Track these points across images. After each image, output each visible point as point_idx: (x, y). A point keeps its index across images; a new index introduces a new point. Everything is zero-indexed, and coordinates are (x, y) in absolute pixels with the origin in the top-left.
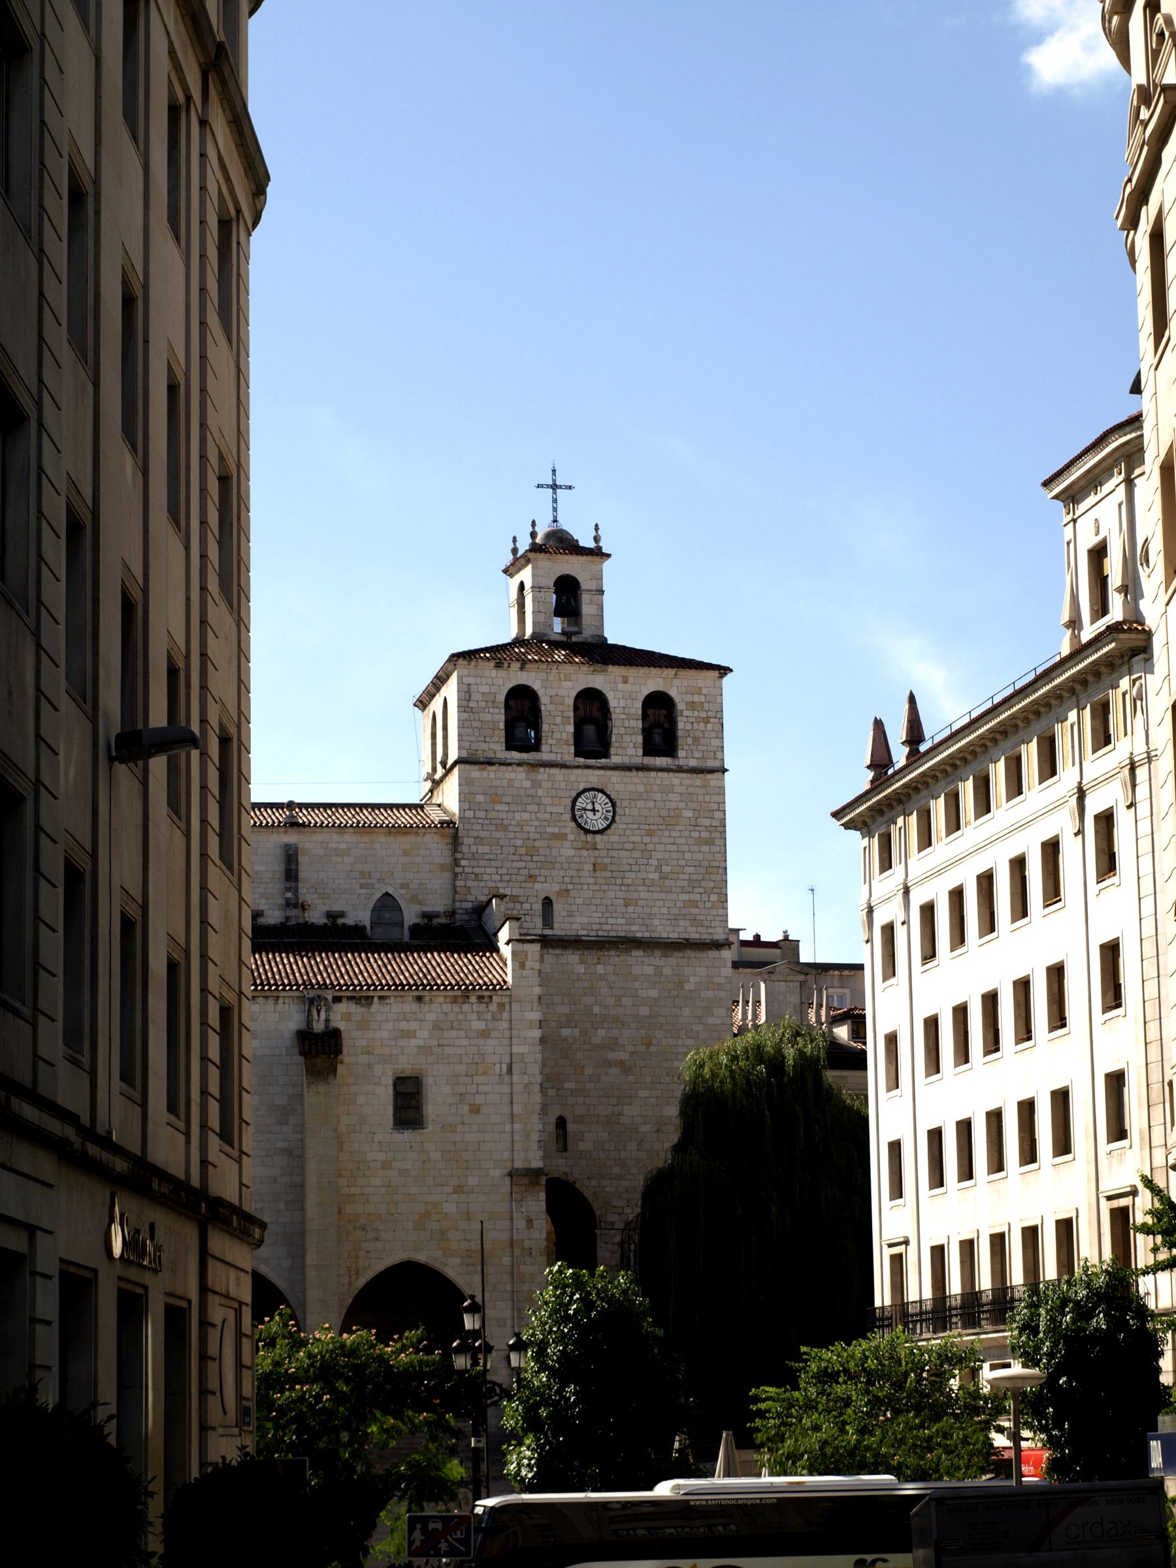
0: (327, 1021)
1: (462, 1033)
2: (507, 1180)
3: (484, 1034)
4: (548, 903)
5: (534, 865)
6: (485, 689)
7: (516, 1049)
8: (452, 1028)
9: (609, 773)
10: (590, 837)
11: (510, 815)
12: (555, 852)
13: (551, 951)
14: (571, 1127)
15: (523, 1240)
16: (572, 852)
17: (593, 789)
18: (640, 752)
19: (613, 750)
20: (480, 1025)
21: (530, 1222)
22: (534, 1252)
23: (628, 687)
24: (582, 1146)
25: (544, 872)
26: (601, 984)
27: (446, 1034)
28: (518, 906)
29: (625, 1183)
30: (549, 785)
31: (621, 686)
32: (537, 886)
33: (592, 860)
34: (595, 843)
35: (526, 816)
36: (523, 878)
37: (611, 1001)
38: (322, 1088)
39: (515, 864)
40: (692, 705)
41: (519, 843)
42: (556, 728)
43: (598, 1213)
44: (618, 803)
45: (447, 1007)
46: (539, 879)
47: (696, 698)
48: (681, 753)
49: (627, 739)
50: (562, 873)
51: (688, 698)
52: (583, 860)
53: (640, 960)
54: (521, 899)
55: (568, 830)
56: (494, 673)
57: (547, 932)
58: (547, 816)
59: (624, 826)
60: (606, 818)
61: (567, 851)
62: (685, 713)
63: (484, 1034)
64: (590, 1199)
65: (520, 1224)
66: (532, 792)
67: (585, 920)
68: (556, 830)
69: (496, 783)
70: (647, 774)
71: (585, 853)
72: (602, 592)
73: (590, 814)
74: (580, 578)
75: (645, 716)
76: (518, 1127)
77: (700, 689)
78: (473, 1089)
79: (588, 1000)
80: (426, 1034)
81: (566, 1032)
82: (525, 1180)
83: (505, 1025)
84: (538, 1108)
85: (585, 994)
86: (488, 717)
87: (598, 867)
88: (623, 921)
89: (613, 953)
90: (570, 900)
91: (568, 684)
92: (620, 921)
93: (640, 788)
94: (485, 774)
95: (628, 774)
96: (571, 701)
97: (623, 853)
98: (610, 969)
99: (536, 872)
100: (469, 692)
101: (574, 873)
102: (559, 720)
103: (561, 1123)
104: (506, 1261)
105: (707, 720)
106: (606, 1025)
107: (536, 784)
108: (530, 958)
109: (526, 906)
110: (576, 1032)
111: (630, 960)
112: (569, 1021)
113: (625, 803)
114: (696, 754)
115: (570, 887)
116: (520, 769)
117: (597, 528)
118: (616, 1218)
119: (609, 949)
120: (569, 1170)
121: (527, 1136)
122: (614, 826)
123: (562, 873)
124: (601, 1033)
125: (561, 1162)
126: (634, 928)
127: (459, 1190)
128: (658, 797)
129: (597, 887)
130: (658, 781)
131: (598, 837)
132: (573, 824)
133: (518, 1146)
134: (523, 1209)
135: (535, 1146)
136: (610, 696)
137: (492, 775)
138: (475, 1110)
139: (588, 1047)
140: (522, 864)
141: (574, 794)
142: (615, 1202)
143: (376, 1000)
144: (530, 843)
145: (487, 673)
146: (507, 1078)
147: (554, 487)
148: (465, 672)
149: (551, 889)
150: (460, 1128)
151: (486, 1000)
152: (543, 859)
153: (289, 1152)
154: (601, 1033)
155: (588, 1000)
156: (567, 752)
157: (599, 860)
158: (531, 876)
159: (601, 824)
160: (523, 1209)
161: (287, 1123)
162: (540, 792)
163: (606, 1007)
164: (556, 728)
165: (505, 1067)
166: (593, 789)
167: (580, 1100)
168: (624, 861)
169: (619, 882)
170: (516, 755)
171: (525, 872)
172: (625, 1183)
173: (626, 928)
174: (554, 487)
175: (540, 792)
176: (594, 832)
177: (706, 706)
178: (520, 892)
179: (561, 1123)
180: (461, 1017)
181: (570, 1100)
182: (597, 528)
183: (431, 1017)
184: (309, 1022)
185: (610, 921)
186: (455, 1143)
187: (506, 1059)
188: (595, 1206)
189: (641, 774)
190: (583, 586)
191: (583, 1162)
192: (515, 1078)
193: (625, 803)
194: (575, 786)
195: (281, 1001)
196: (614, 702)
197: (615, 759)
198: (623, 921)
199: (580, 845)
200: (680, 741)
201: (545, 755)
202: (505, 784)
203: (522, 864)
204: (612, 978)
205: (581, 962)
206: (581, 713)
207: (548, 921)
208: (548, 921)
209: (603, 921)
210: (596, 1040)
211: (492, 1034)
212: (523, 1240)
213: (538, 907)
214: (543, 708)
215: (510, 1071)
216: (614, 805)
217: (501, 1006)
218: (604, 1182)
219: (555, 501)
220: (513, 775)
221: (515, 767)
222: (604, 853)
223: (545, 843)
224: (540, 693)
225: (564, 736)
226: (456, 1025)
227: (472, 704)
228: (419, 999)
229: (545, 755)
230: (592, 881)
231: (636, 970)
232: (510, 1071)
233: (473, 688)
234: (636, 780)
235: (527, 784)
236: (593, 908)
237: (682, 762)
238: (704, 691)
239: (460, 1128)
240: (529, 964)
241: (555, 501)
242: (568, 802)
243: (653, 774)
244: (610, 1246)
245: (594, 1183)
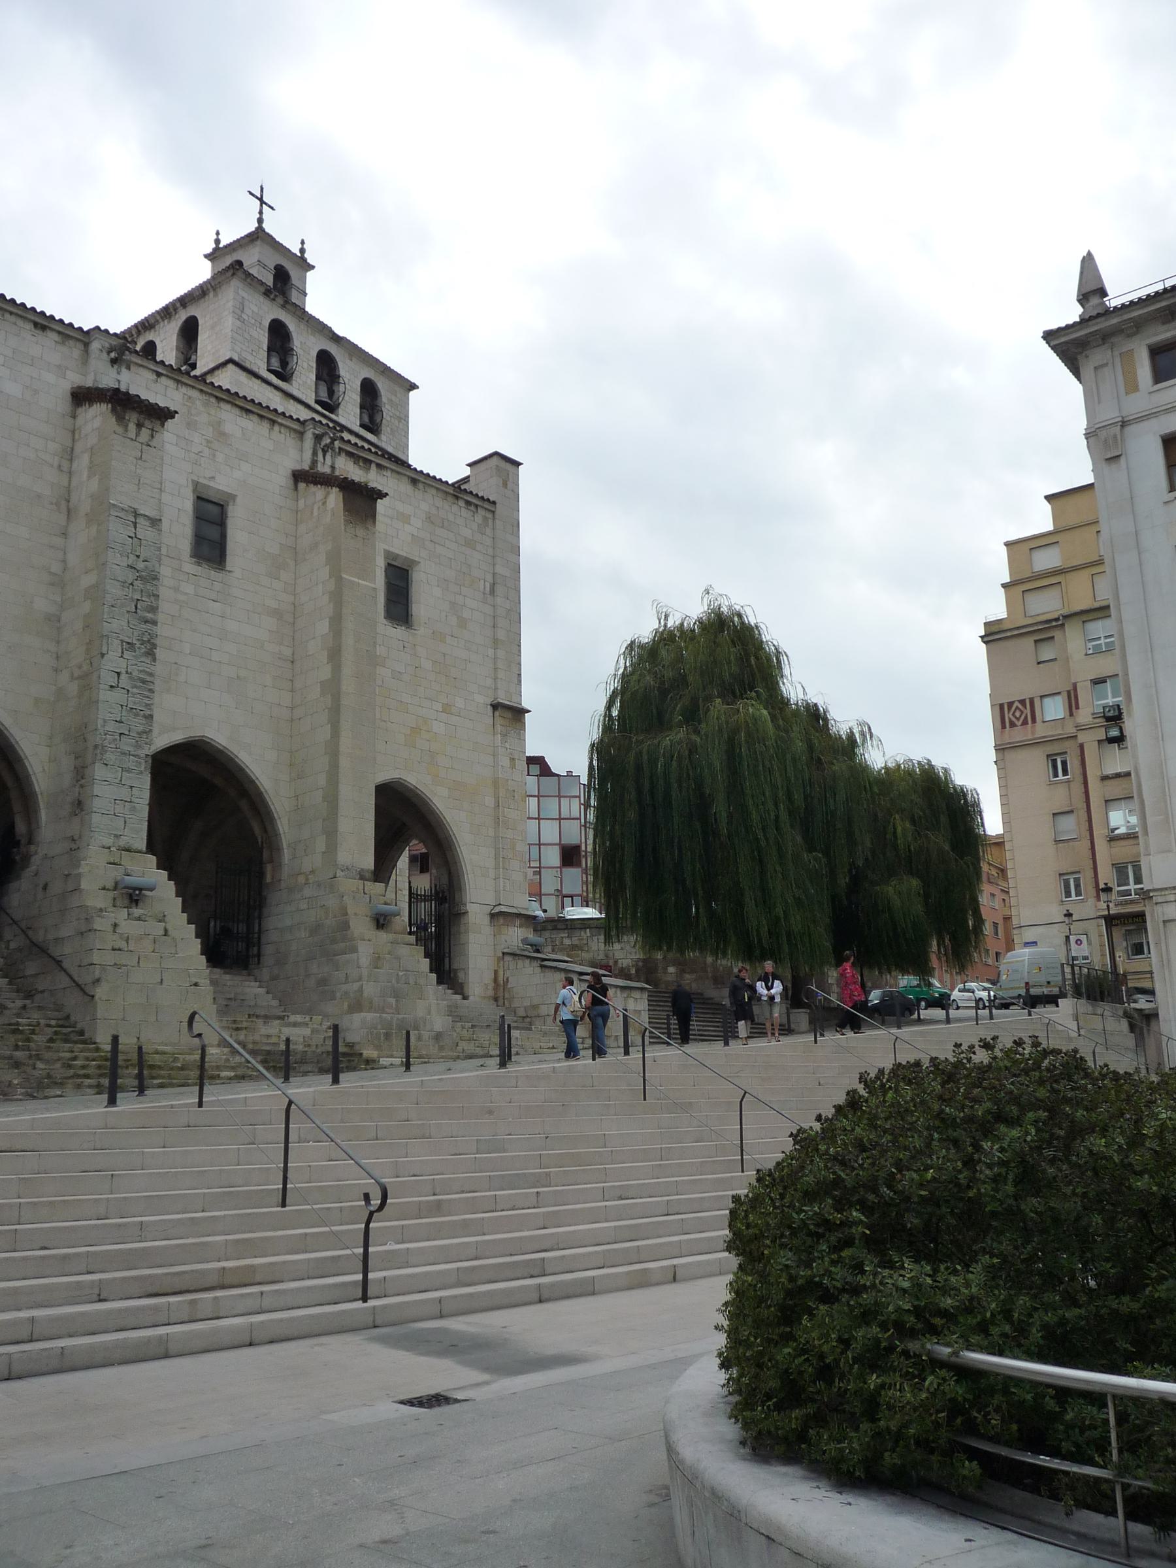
0: (333, 467)
2: (490, 708)
3: (470, 544)
19: (340, 411)
20: (467, 533)
31: (348, 361)
38: (360, 532)
40: (390, 400)
45: (439, 502)
47: (393, 398)
48: (383, 437)
56: (262, 299)
63: (470, 544)
65: (505, 762)
72: (305, 295)
76: (501, 653)
80: (420, 525)
82: (509, 715)
83: (489, 542)
94: (251, 384)
100: (243, 304)
116: (277, 393)
127: (447, 709)
133: (501, 674)
134: (507, 745)
136: (340, 364)
137: (256, 387)
143: (373, 466)
148: (241, 285)
150: (449, 639)
151: (472, 508)
153: (277, 613)
160: (507, 745)
161: (278, 579)
165: (488, 585)
174: (261, 200)
180: (451, 518)
184: (314, 462)
187: (489, 578)
195: (276, 428)
200: (383, 427)
215: (492, 592)
217: (485, 519)
224: (294, 335)
226: (446, 523)
227: (245, 317)
228: (414, 482)
232: (492, 592)
233: (246, 303)
239: (449, 639)
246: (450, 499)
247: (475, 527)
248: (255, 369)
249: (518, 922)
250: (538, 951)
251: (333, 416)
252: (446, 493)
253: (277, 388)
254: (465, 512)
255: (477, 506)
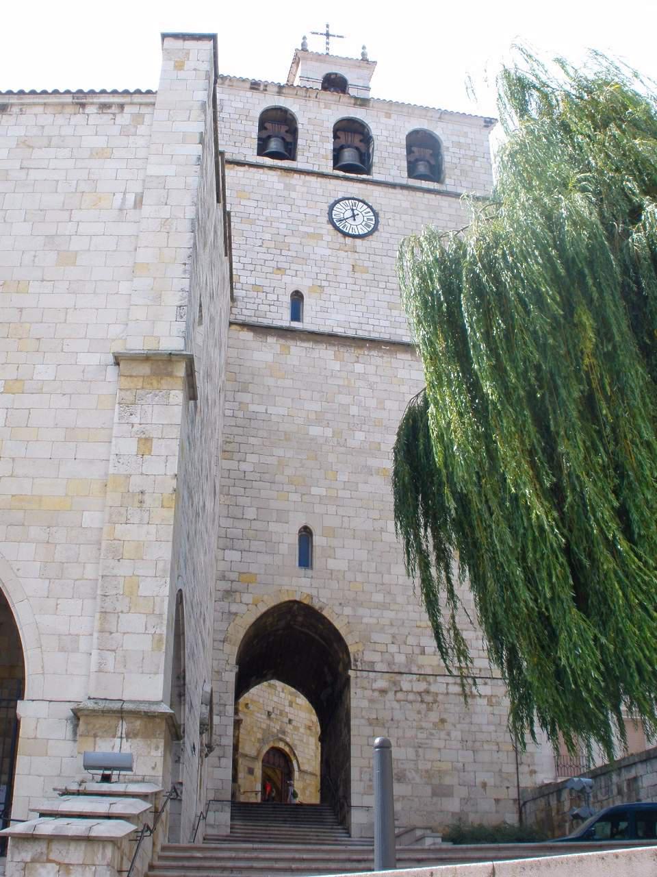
1: (66, 152)
2: (112, 371)
4: (297, 299)
5: (282, 258)
6: (240, 105)
7: (152, 170)
8: (49, 146)
9: (370, 187)
10: (349, 240)
11: (258, 211)
12: (307, 249)
13: (299, 343)
14: (318, 540)
15: (128, 476)
16: (328, 252)
17: (353, 199)
18: (405, 174)
19: (374, 169)
20: (100, 142)
21: (145, 442)
22: (146, 497)
23: (391, 122)
24: (332, 564)
25: (294, 267)
26: (359, 383)
27: (37, 153)
28: (262, 295)
29: (389, 615)
30: (305, 189)
31: (383, 120)
32: (286, 279)
33: (351, 262)
34: (355, 246)
35: (277, 214)
36: (270, 270)
37: (372, 403)
39: (260, 256)
41: (268, 236)
42: (313, 144)
43: (352, 649)
44: (381, 215)
45: (47, 118)
46: (288, 272)
47: (462, 140)
48: (447, 181)
49: (389, 158)
50: (315, 269)
51: (455, 139)
52: (340, 260)
53: (407, 364)
54: (265, 289)
55: (324, 232)
56: (249, 94)
57: (295, 325)
58: (302, 217)
59: (388, 235)
60: (367, 225)
61: (322, 250)
62: (451, 150)
64: (343, 632)
65: (129, 446)
66: (286, 193)
67: (341, 317)
68: (311, 230)
69: (243, 181)
70: (412, 193)
71: (343, 254)
73: (351, 221)
74: (347, 77)
75: (409, 151)
77: (466, 133)
78: (70, 228)
79: (344, 399)
81: (315, 431)
82: (145, 369)
84: (183, 254)
85: (340, 393)
86: (241, 127)
87: (357, 268)
88: (387, 323)
89: (374, 353)
90: (324, 296)
91: (329, 112)
92: (382, 323)
93: (405, 204)
95: (391, 190)
96: (331, 126)
97: (385, 259)
98: (371, 369)
99: (286, 266)
101: (331, 272)
102: (317, 138)
103: (306, 535)
104: (92, 519)
105: (474, 158)
106: (366, 427)
107: (288, 187)
108: (192, 56)
109: (272, 297)
110: (329, 432)
111: (395, 363)
112: (319, 419)
113: (388, 215)
114: (464, 184)
115: (324, 283)
116: (272, 173)
117: (364, 48)
118: (376, 657)
119: (369, 349)
120: (314, 593)
121: (158, 298)
122: (376, 234)
123: (315, 269)
124: (360, 436)
125: (305, 581)
126: (400, 332)
128: (426, 214)
129: (357, 288)
130: (425, 201)
131: (358, 241)
132: (330, 227)
134: (135, 420)
135: (171, 313)
138: (68, 258)
139: (343, 449)
140: (270, 257)
141: (332, 201)
142: (375, 637)
144: (280, 238)
145: (242, 93)
146: (133, 215)
147: (328, 35)
149: (303, 284)
151: (114, 109)
152: (294, 254)
154: (360, 436)
155: (344, 399)
156: (327, 166)
157: (360, 263)
158: (279, 269)
159: (362, 230)
160: (135, 420)
162: (293, 195)
163: (366, 409)
164: (313, 144)
165: (131, 198)
166: (353, 199)
167: (332, 509)
168: (388, 267)
169: (382, 285)
170: (268, 161)
171: (274, 264)
172: (391, 615)
173: (393, 331)
174: (328, 35)
175: (293, 195)
176: (354, 237)
177: (473, 147)
178: (266, 282)
179: (306, 535)
180: (67, 131)
181: (318, 509)
182: (364, 48)
183: (20, 131)
185: (371, 321)
186: (21, 310)
188: (349, 640)
189: (405, 192)
190: (349, 82)
191: (334, 585)
192: (146, 210)
193: (388, 215)
194: (333, 193)
196: (374, 130)
197: (376, 176)
198: (387, 323)
199: (338, 246)
201: (300, 163)
202: (254, 183)
203: (270, 257)
204: (373, 379)
205: (336, 358)
206: (342, 141)
207: (296, 314)
208: (296, 314)
209: (363, 320)
210: (352, 443)
211: (117, 154)
212: (128, 476)
213: (287, 300)
214: (300, 126)
215: (139, 203)
216: (376, 215)
218: (361, 611)
219: (327, 43)
220: (263, 177)
221: (266, 169)
222: (362, 257)
223: (297, 240)
225: (322, 152)
226: (55, 141)
229: (300, 163)
230: (350, 280)
231: (402, 374)
232: (139, 203)
234: (400, 198)
235: (281, 186)
236: (351, 307)
237: (450, 189)
238: (470, 135)
240: (190, 64)
241: (327, 43)
242: (326, 208)
243: (419, 194)
244: (368, 693)
245: (348, 611)
246: (69, 110)
247: (116, 130)
248: (241, 158)
249: (123, 727)
250: (106, 779)
251: (364, 176)
252: (63, 105)
253: (271, 168)
254: (106, 118)
255: (122, 106)
